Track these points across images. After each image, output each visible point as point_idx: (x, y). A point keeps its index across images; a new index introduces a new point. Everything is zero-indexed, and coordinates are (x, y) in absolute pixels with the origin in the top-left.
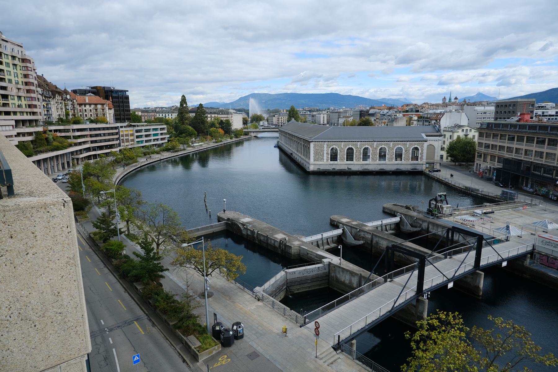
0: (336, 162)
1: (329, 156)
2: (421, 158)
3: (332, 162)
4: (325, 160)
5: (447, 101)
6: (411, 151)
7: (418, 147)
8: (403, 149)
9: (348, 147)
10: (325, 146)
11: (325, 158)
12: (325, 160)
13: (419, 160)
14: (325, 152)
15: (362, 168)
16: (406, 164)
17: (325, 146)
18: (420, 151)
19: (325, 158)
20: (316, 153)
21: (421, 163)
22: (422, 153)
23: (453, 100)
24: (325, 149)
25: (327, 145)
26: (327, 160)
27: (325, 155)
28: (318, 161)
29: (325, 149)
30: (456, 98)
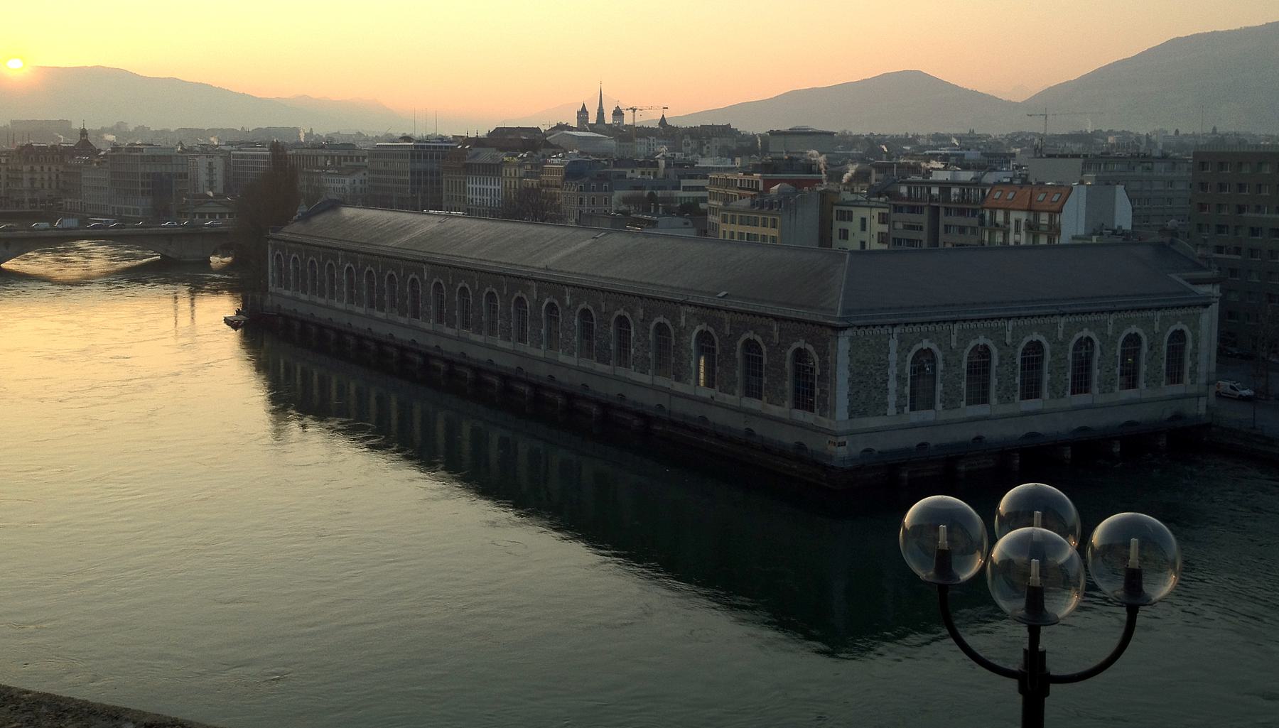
0: (928, 415)
1: (907, 390)
2: (1193, 372)
3: (916, 417)
4: (892, 410)
5: (592, 119)
6: (1165, 348)
7: (1185, 328)
8: (1144, 339)
10: (893, 344)
11: (892, 399)
12: (892, 410)
13: (1187, 379)
14: (893, 371)
15: (1021, 432)
16: (1149, 401)
17: (893, 344)
18: (1189, 346)
19: (892, 399)
20: (857, 380)
21: (1193, 390)
22: (1195, 354)
23: (609, 119)
24: (893, 357)
25: (901, 341)
26: (900, 407)
27: (892, 385)
28: (864, 414)
29: (893, 357)
30: (618, 113)
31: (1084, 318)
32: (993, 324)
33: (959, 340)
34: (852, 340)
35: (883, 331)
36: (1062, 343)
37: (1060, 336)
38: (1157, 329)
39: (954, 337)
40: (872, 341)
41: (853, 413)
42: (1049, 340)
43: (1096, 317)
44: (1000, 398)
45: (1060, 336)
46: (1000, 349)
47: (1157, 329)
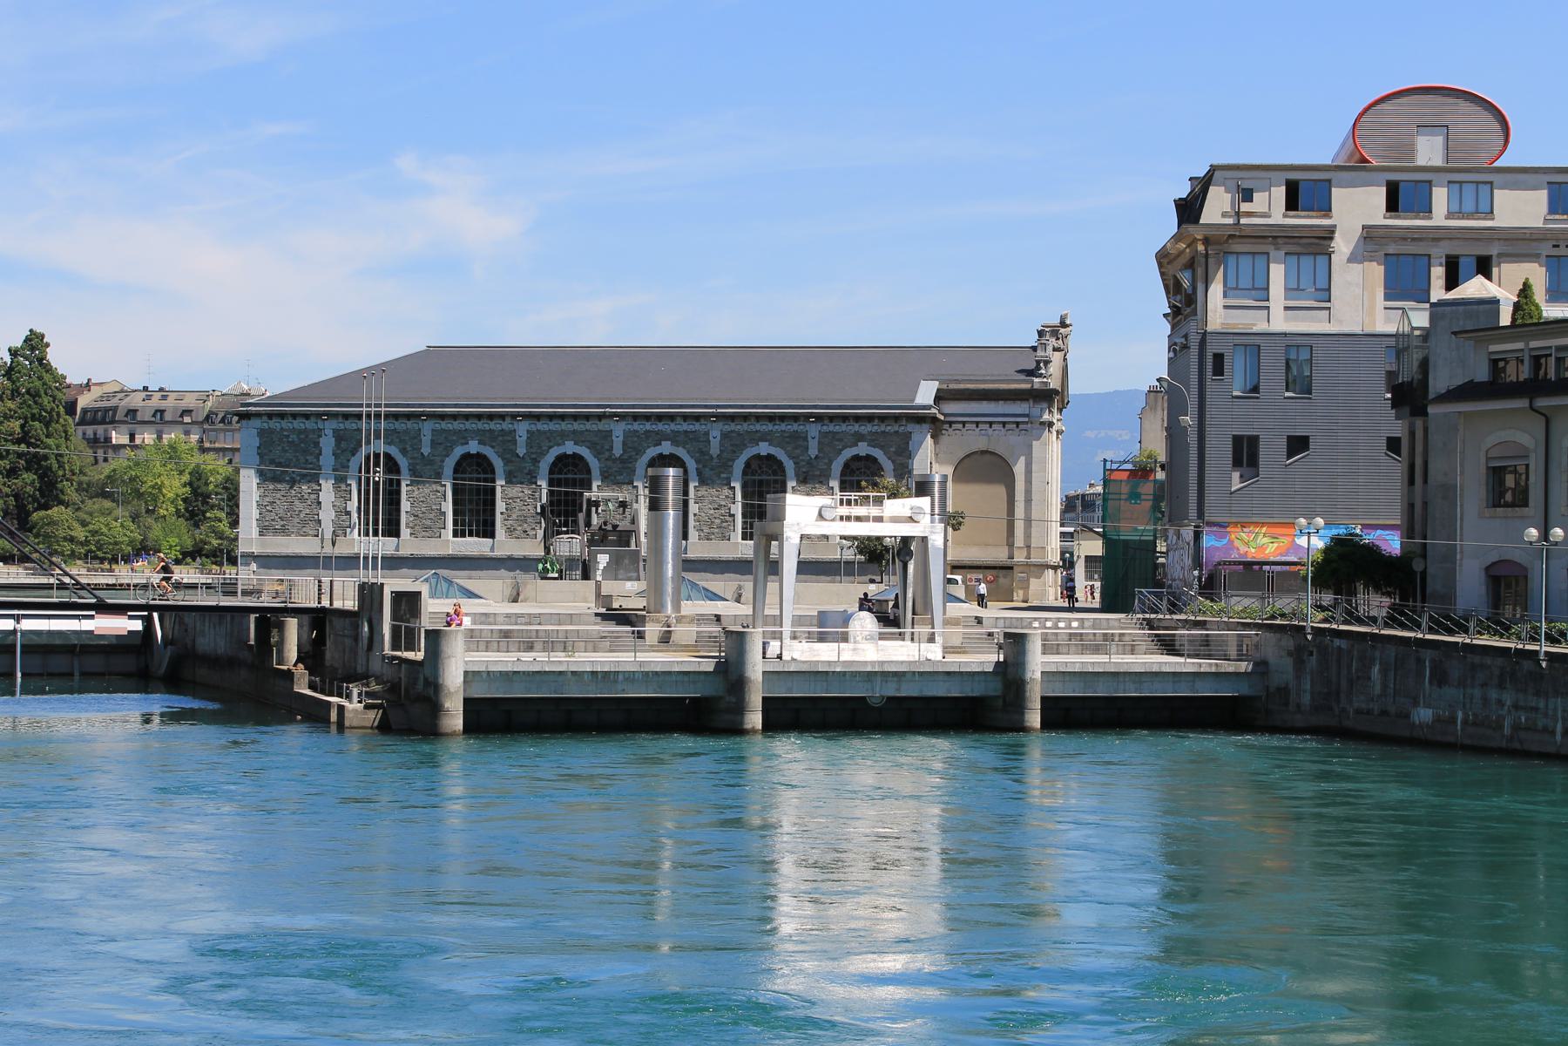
9: (459, 451)
28: (284, 531)
31: (660, 426)
32: (493, 425)
33: (434, 444)
34: (262, 433)
35: (310, 424)
36: (621, 460)
37: (618, 451)
38: (813, 451)
39: (426, 439)
40: (293, 437)
41: (263, 531)
42: (597, 454)
43: (685, 427)
44: (510, 531)
45: (618, 451)
46: (507, 462)
47: (813, 451)
